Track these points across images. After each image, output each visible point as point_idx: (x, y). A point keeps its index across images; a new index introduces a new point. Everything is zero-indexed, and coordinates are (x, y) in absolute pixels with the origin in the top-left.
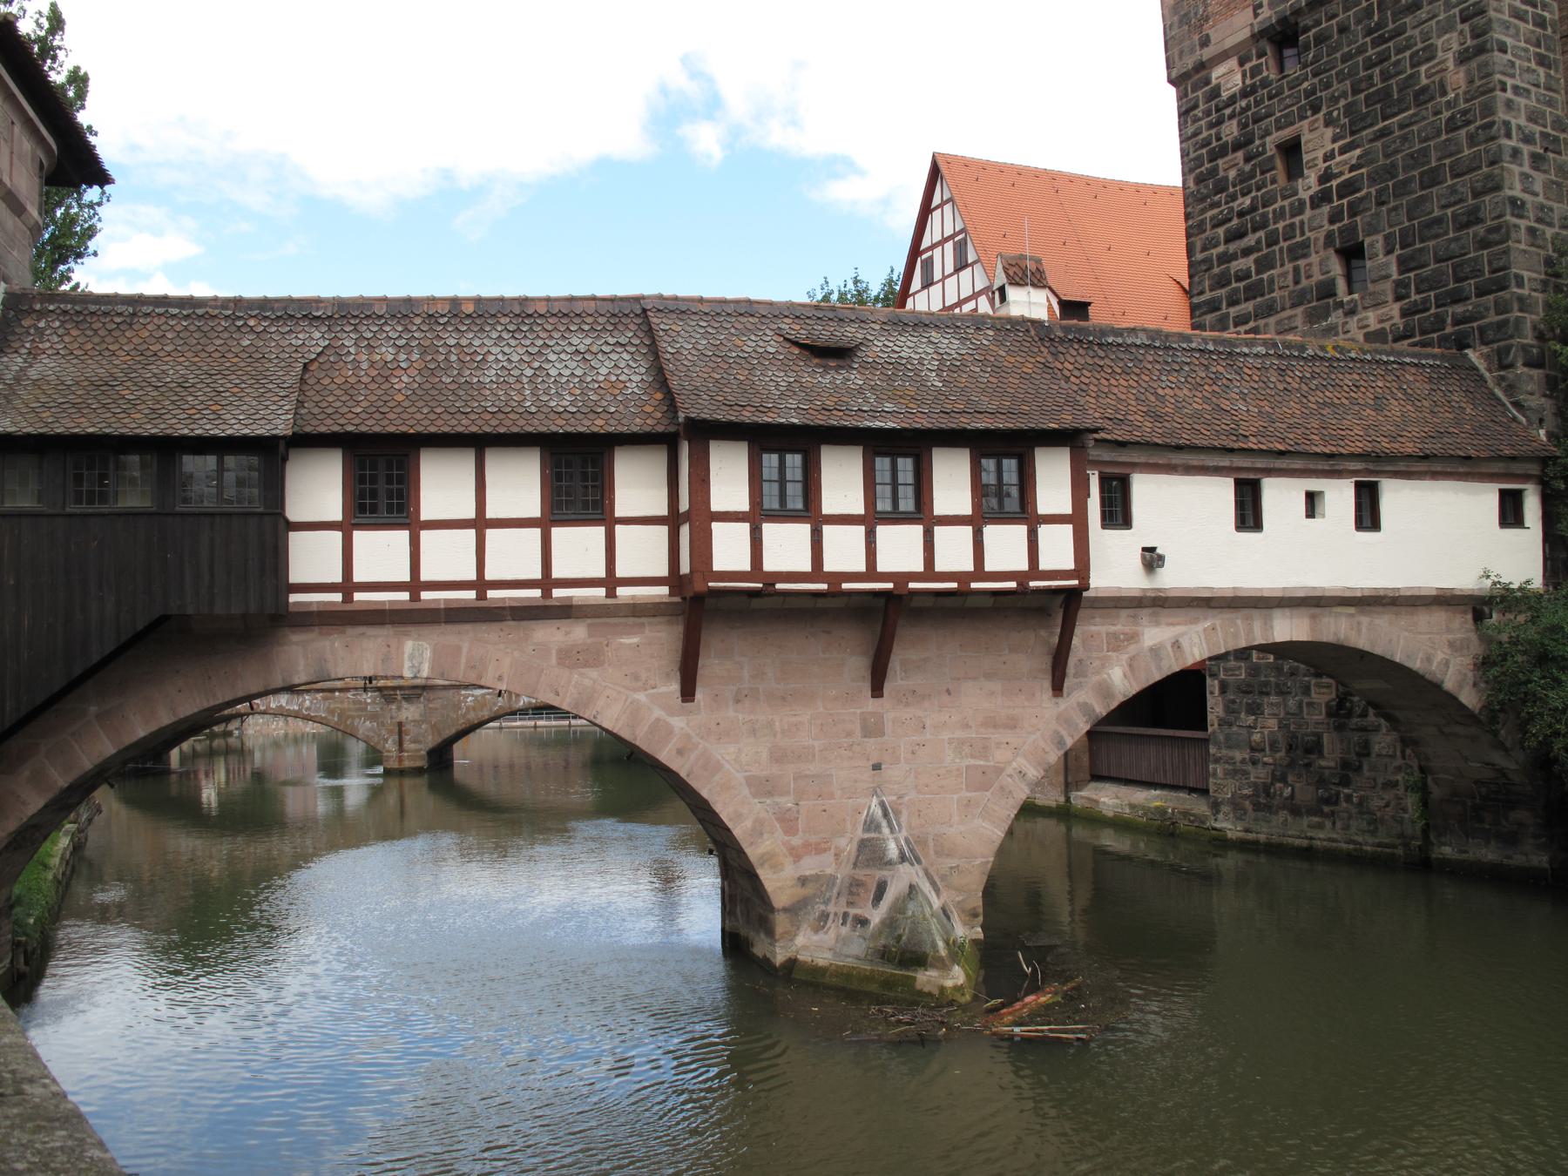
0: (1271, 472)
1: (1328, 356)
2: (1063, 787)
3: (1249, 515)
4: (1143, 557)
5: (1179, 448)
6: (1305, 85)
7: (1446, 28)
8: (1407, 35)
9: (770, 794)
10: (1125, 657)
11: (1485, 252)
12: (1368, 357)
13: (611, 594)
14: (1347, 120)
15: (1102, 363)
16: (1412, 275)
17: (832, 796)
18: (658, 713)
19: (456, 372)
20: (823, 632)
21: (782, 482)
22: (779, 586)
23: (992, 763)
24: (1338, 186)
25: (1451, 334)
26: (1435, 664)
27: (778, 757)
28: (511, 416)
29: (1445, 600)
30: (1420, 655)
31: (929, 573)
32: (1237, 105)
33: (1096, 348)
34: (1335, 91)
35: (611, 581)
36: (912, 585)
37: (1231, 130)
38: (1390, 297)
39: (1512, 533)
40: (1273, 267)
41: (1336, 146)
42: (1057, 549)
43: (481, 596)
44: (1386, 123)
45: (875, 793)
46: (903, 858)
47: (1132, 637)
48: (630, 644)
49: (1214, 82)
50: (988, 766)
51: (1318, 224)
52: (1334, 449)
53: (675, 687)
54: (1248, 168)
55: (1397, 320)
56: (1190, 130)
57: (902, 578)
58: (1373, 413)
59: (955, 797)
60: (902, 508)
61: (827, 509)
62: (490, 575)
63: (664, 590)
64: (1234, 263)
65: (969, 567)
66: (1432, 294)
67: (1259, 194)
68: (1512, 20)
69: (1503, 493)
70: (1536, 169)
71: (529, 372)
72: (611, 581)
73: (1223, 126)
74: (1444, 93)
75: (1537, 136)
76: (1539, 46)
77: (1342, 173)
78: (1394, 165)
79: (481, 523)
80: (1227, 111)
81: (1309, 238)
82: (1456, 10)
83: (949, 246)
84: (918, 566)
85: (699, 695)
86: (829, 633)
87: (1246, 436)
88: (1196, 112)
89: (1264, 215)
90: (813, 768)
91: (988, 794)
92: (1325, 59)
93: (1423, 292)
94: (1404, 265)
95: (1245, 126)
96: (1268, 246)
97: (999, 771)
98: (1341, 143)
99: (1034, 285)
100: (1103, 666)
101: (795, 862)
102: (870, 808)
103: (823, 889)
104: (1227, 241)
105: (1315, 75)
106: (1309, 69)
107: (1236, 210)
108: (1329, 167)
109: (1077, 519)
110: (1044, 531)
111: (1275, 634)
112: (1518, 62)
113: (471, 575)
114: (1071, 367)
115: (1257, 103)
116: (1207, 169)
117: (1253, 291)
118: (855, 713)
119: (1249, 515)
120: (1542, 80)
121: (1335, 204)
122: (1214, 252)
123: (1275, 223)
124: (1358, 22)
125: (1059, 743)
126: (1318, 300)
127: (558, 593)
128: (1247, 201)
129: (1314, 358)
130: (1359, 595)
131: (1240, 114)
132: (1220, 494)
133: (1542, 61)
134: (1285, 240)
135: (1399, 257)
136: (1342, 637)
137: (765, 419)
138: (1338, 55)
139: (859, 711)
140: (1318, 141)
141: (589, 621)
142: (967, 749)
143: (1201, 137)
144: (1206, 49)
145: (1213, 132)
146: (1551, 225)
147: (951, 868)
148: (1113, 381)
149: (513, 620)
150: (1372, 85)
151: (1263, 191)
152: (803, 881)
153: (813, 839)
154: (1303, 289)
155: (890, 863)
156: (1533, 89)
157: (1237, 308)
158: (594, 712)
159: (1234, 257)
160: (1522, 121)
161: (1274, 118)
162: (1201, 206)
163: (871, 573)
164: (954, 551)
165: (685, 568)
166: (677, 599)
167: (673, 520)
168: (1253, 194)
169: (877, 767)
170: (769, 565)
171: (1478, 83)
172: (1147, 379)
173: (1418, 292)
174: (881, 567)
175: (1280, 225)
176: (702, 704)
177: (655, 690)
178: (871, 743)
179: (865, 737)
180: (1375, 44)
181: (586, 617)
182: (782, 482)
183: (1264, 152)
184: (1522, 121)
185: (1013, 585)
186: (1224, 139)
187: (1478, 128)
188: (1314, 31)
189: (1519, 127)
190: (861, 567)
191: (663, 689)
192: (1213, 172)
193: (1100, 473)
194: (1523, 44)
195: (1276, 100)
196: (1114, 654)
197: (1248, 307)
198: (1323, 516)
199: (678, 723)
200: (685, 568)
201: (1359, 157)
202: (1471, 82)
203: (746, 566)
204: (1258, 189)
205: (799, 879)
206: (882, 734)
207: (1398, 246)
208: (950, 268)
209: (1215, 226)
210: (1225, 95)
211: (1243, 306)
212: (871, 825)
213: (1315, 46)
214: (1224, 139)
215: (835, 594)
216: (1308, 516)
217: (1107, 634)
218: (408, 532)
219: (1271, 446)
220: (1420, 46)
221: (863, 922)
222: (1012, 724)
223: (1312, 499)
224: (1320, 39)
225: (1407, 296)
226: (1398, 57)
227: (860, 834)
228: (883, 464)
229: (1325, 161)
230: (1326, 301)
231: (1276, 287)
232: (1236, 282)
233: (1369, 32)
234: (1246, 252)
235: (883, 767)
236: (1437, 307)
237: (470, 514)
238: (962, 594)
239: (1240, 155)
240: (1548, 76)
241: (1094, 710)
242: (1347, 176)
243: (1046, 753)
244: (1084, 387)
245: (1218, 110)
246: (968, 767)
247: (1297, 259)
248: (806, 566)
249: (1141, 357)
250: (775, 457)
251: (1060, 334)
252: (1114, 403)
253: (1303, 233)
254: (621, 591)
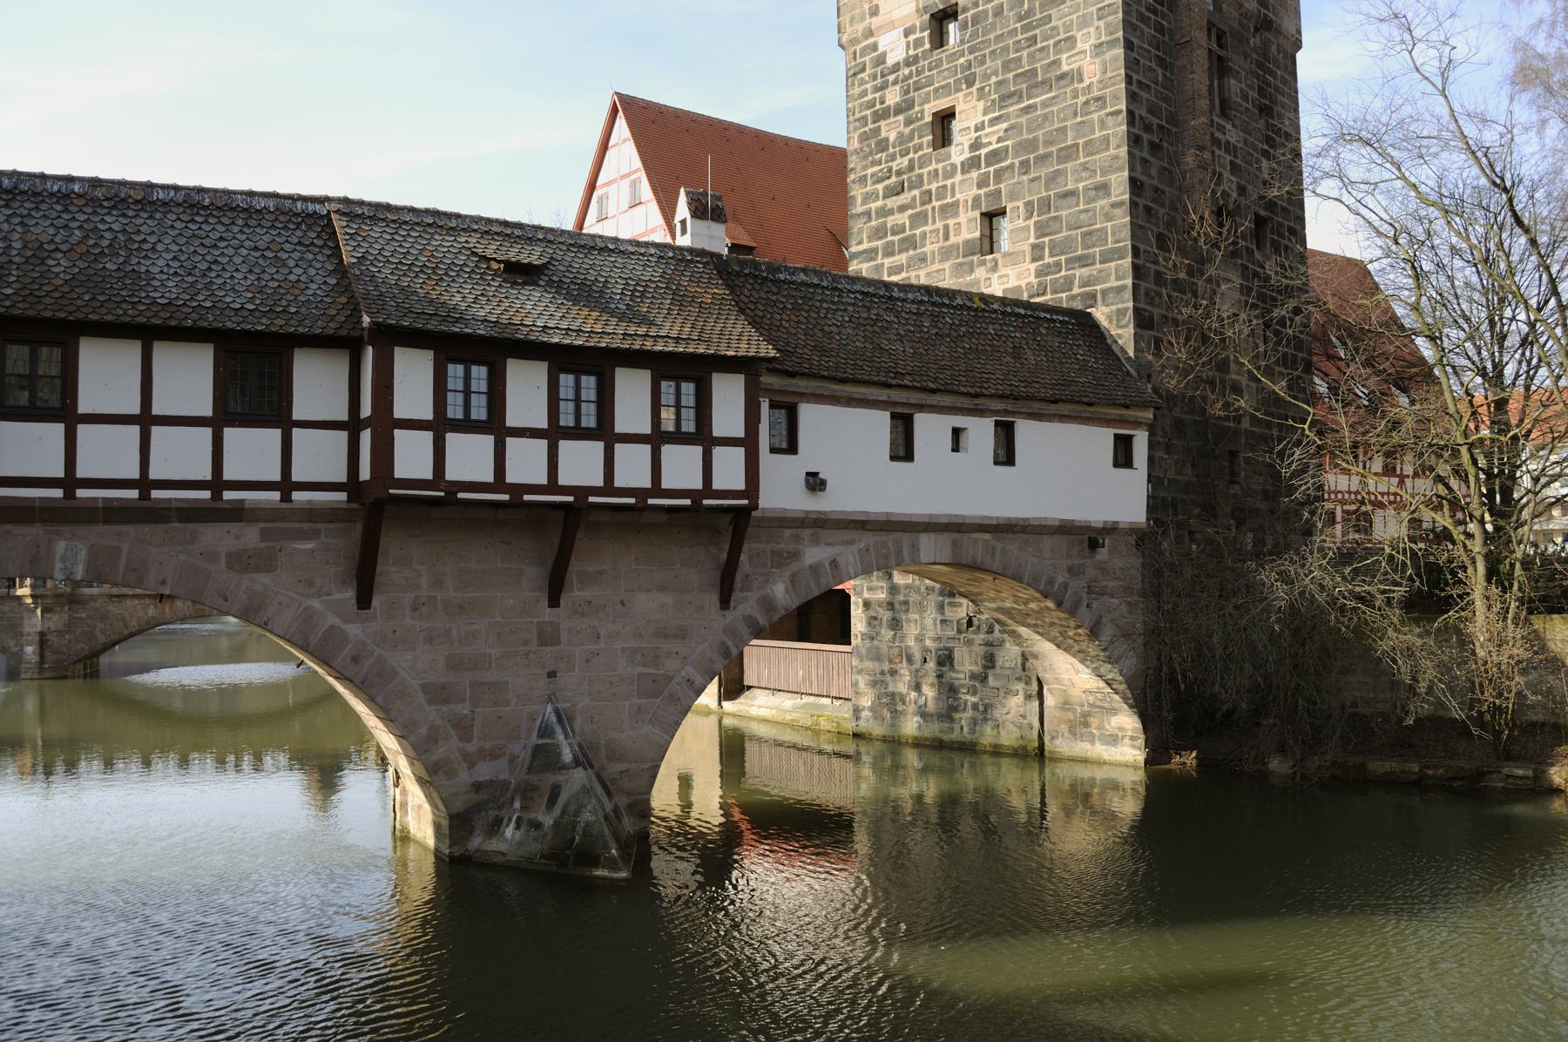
0: (922, 408)
1: (975, 306)
2: (716, 697)
3: (903, 450)
4: (807, 482)
5: (843, 381)
6: (962, 60)
7: (1084, 23)
8: (1052, 24)
9: (446, 701)
10: (787, 574)
11: (1110, 224)
12: (1009, 310)
13: (286, 498)
14: (997, 96)
15: (774, 298)
16: (1046, 239)
17: (507, 703)
18: (332, 620)
19: (121, 260)
20: (503, 542)
21: (467, 392)
22: (461, 495)
23: (662, 672)
24: (986, 155)
25: (1079, 295)
26: (1056, 586)
27: (455, 664)
28: (184, 310)
29: (1066, 529)
30: (1044, 578)
32: (901, 72)
33: (770, 284)
34: (987, 69)
35: (286, 485)
36: (592, 499)
37: (893, 97)
38: (1028, 258)
39: (1124, 472)
40: (926, 223)
41: (987, 118)
42: (729, 470)
43: (145, 496)
44: (1031, 102)
45: (549, 700)
46: (577, 763)
47: (794, 555)
48: (305, 550)
49: (881, 49)
50: (658, 675)
51: (966, 190)
52: (979, 390)
53: (350, 594)
54: (907, 131)
55: (1033, 279)
56: (857, 90)
57: (581, 492)
58: (1012, 361)
59: (627, 703)
60: (584, 424)
61: (511, 421)
62: (154, 474)
63: (342, 496)
64: (890, 218)
65: (647, 484)
66: (1063, 258)
67: (916, 156)
68: (1138, 23)
69: (1117, 436)
70: (1153, 156)
71: (204, 266)
72: (286, 485)
73: (887, 91)
74: (1081, 80)
75: (1155, 127)
76: (1158, 50)
77: (990, 143)
78: (1035, 139)
79: (146, 420)
80: (891, 78)
81: (958, 201)
82: (1094, 8)
83: (626, 182)
84: (600, 482)
85: (375, 602)
86: (508, 543)
87: (902, 374)
88: (863, 75)
89: (920, 176)
90: (488, 677)
91: (658, 701)
92: (980, 39)
93: (1056, 255)
94: (1041, 230)
95: (907, 92)
96: (923, 204)
97: (669, 679)
98: (991, 116)
99: (713, 219)
100: (767, 582)
101: (469, 768)
102: (544, 715)
103: (497, 794)
104: (885, 197)
105: (970, 53)
106: (966, 46)
107: (895, 169)
108: (979, 137)
109: (749, 443)
110: (718, 452)
111: (921, 557)
112: (1142, 61)
113: (134, 474)
114: (746, 300)
115: (919, 73)
116: (870, 130)
117: (910, 243)
118: (532, 622)
119: (903, 450)
120: (1160, 79)
121: (983, 171)
122: (873, 206)
123: (929, 184)
124: (1012, 9)
125: (725, 652)
126: (964, 256)
127: (228, 495)
128: (906, 163)
129: (962, 307)
130: (995, 523)
131: (903, 81)
132: (878, 424)
133: (1160, 61)
134: (937, 200)
135: (1036, 223)
136: (979, 560)
137: (453, 329)
138: (992, 36)
139: (535, 620)
140: (970, 114)
141: (262, 525)
142: (638, 657)
143: (866, 99)
144: (874, 18)
145: (877, 95)
146: (1162, 205)
147: (622, 772)
148: (785, 317)
149: (180, 522)
150: (1021, 67)
151: (920, 153)
152: (477, 787)
153: (488, 745)
154: (952, 246)
155: (565, 767)
156: (1153, 86)
157: (891, 259)
158: (265, 619)
159: (891, 212)
160: (1144, 113)
161: (932, 87)
162: (864, 163)
163: (553, 486)
164: (633, 468)
165: (365, 474)
166: (354, 506)
167: (352, 426)
168: (911, 155)
169: (552, 674)
170: (452, 474)
171: (1109, 74)
172: (815, 316)
173: (1051, 256)
174: (562, 481)
175: (934, 186)
176: (378, 611)
177: (330, 597)
178: (548, 651)
179: (541, 645)
180: (1025, 29)
181: (258, 520)
182: (467, 392)
183: (922, 118)
184: (1144, 113)
185: (687, 502)
186: (887, 103)
187: (1108, 115)
188: (972, 12)
189: (1141, 117)
190: (543, 480)
191: (338, 596)
192: (877, 131)
193: (770, 401)
194: (1146, 46)
195: (935, 72)
196: (778, 571)
197: (902, 258)
198: (967, 450)
199: (354, 630)
200: (365, 474)
201: (1006, 130)
202: (1105, 72)
203: (427, 473)
204: (916, 152)
205: (473, 785)
206: (558, 643)
207: (1035, 213)
208: (625, 205)
209: (874, 183)
210: (890, 61)
211: (896, 258)
212: (545, 732)
213: (972, 26)
214: (887, 103)
215: (516, 504)
216: (953, 450)
217: (772, 552)
218: (63, 425)
219: (925, 384)
220: (1062, 36)
221: (537, 825)
222: (681, 634)
223: (957, 433)
224: (976, 20)
225: (1041, 258)
226: (1044, 44)
227: (534, 739)
228: (566, 380)
229: (976, 132)
230: (971, 258)
231: (928, 242)
232: (892, 235)
233: (1020, 19)
234: (902, 208)
235: (558, 674)
236: (1067, 270)
237: (134, 408)
238: (641, 508)
239: (901, 118)
240: (1164, 75)
241: (758, 623)
242: (995, 146)
243: (713, 662)
244: (758, 320)
245: (882, 76)
246: (639, 675)
247: (947, 218)
248: (488, 476)
249: (810, 296)
250: (460, 369)
251: (736, 268)
252: (785, 336)
253: (953, 195)
254: (297, 496)
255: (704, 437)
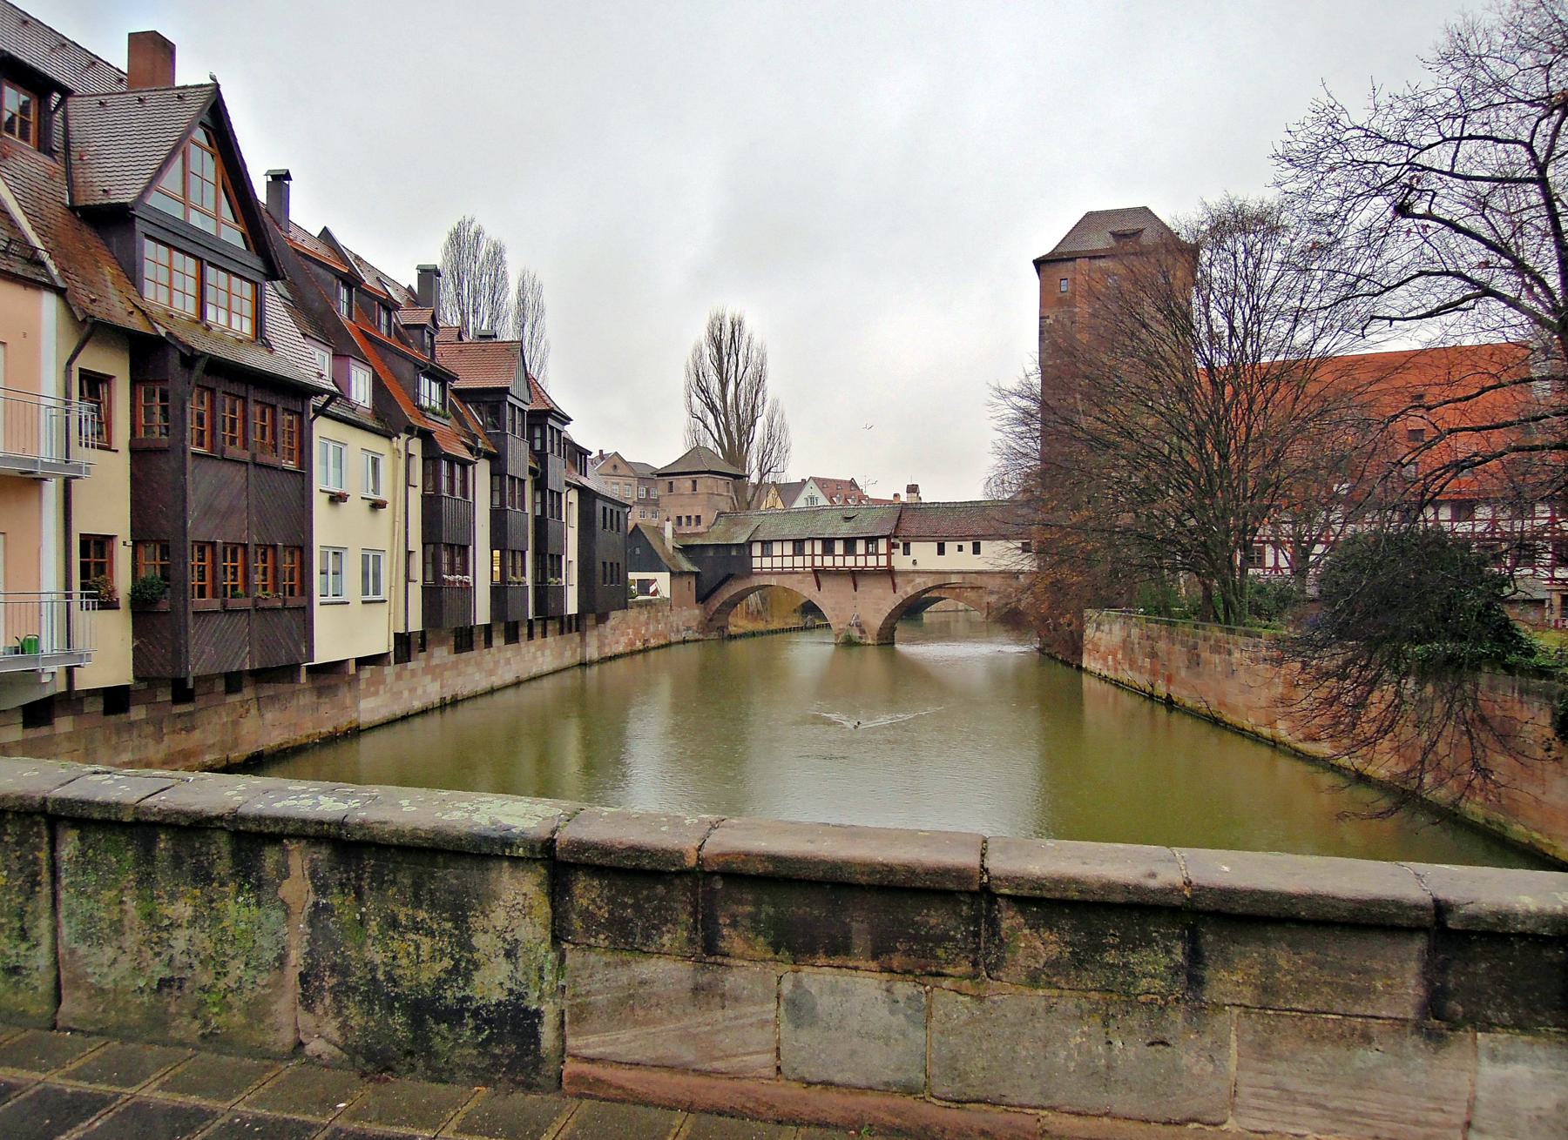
3: (941, 551)
31: (856, 566)
42: (883, 561)
79: (783, 556)
119: (941, 551)
164: (861, 562)
255: (877, 554)
